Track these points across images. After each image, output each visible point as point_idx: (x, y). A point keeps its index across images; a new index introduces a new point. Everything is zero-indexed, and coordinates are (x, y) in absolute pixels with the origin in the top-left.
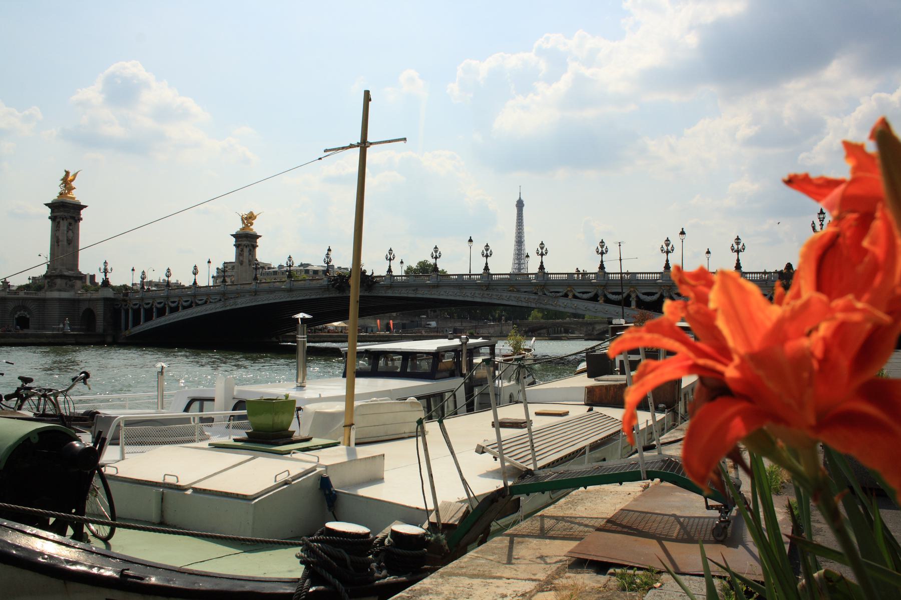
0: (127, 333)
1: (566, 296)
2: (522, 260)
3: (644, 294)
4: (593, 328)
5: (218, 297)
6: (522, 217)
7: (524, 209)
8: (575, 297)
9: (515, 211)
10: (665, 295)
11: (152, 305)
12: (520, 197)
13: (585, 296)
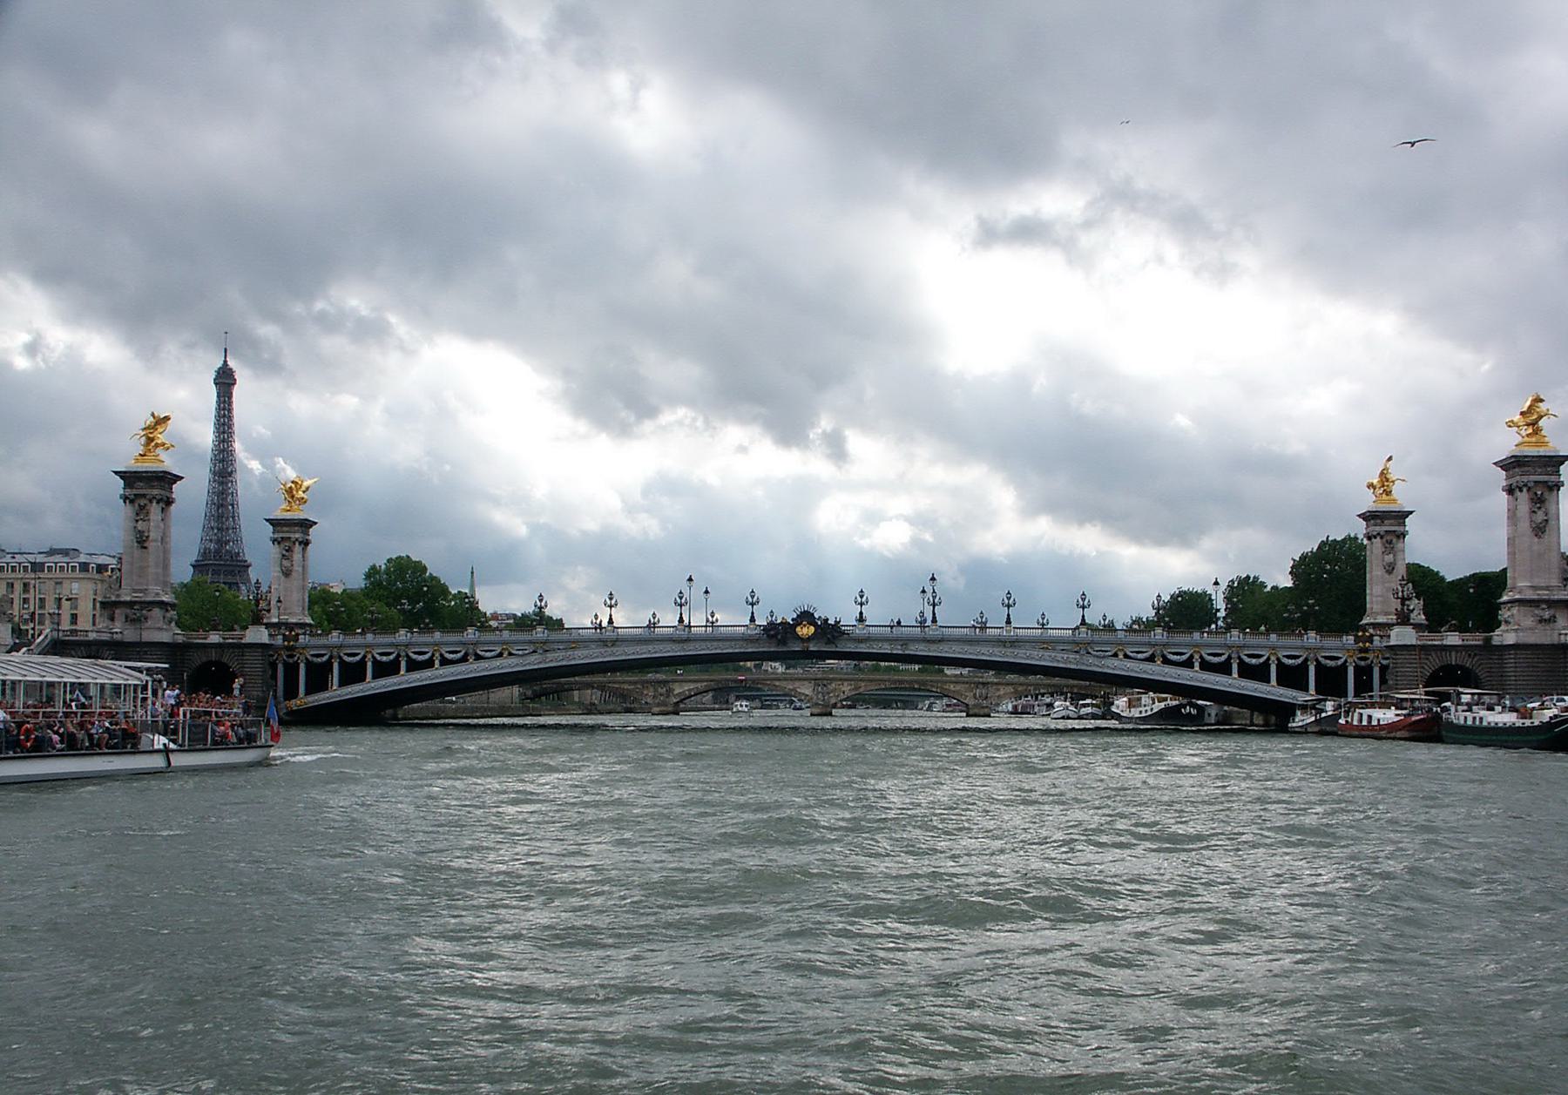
0: (293, 701)
1: (1115, 655)
2: (227, 519)
3: (1209, 654)
4: (670, 691)
5: (531, 648)
6: (230, 411)
7: (236, 391)
8: (1126, 656)
9: (213, 391)
10: (1233, 656)
11: (365, 657)
12: (225, 362)
13: (1140, 656)
